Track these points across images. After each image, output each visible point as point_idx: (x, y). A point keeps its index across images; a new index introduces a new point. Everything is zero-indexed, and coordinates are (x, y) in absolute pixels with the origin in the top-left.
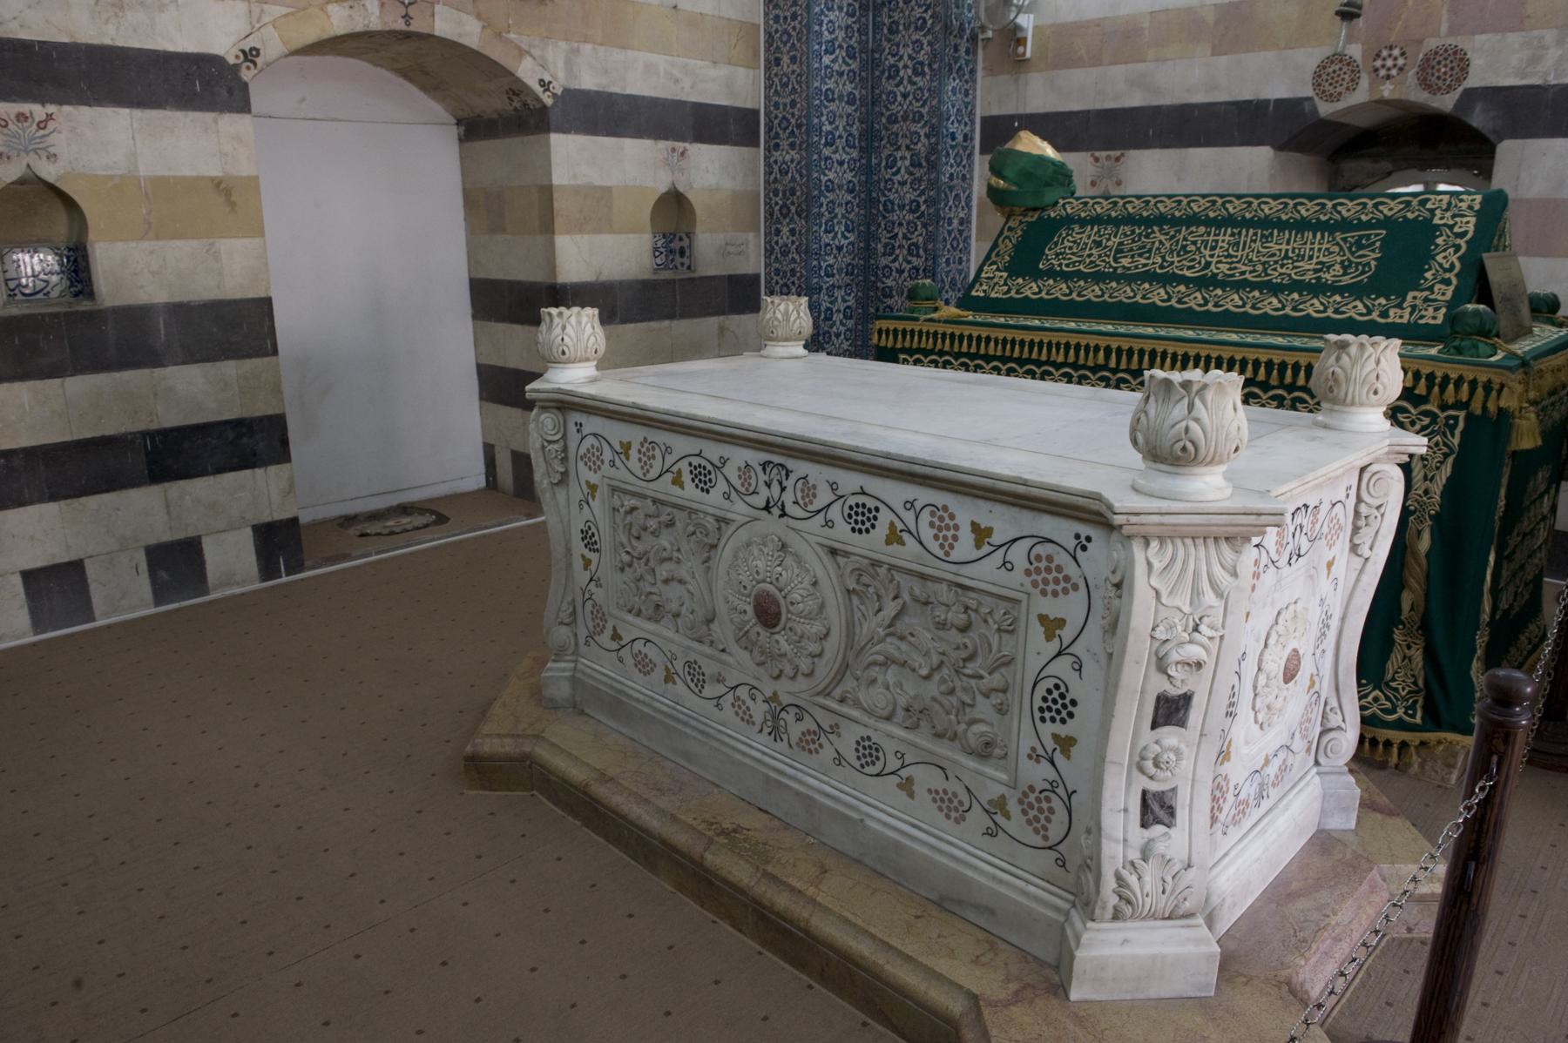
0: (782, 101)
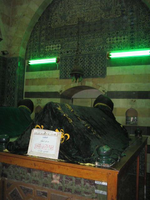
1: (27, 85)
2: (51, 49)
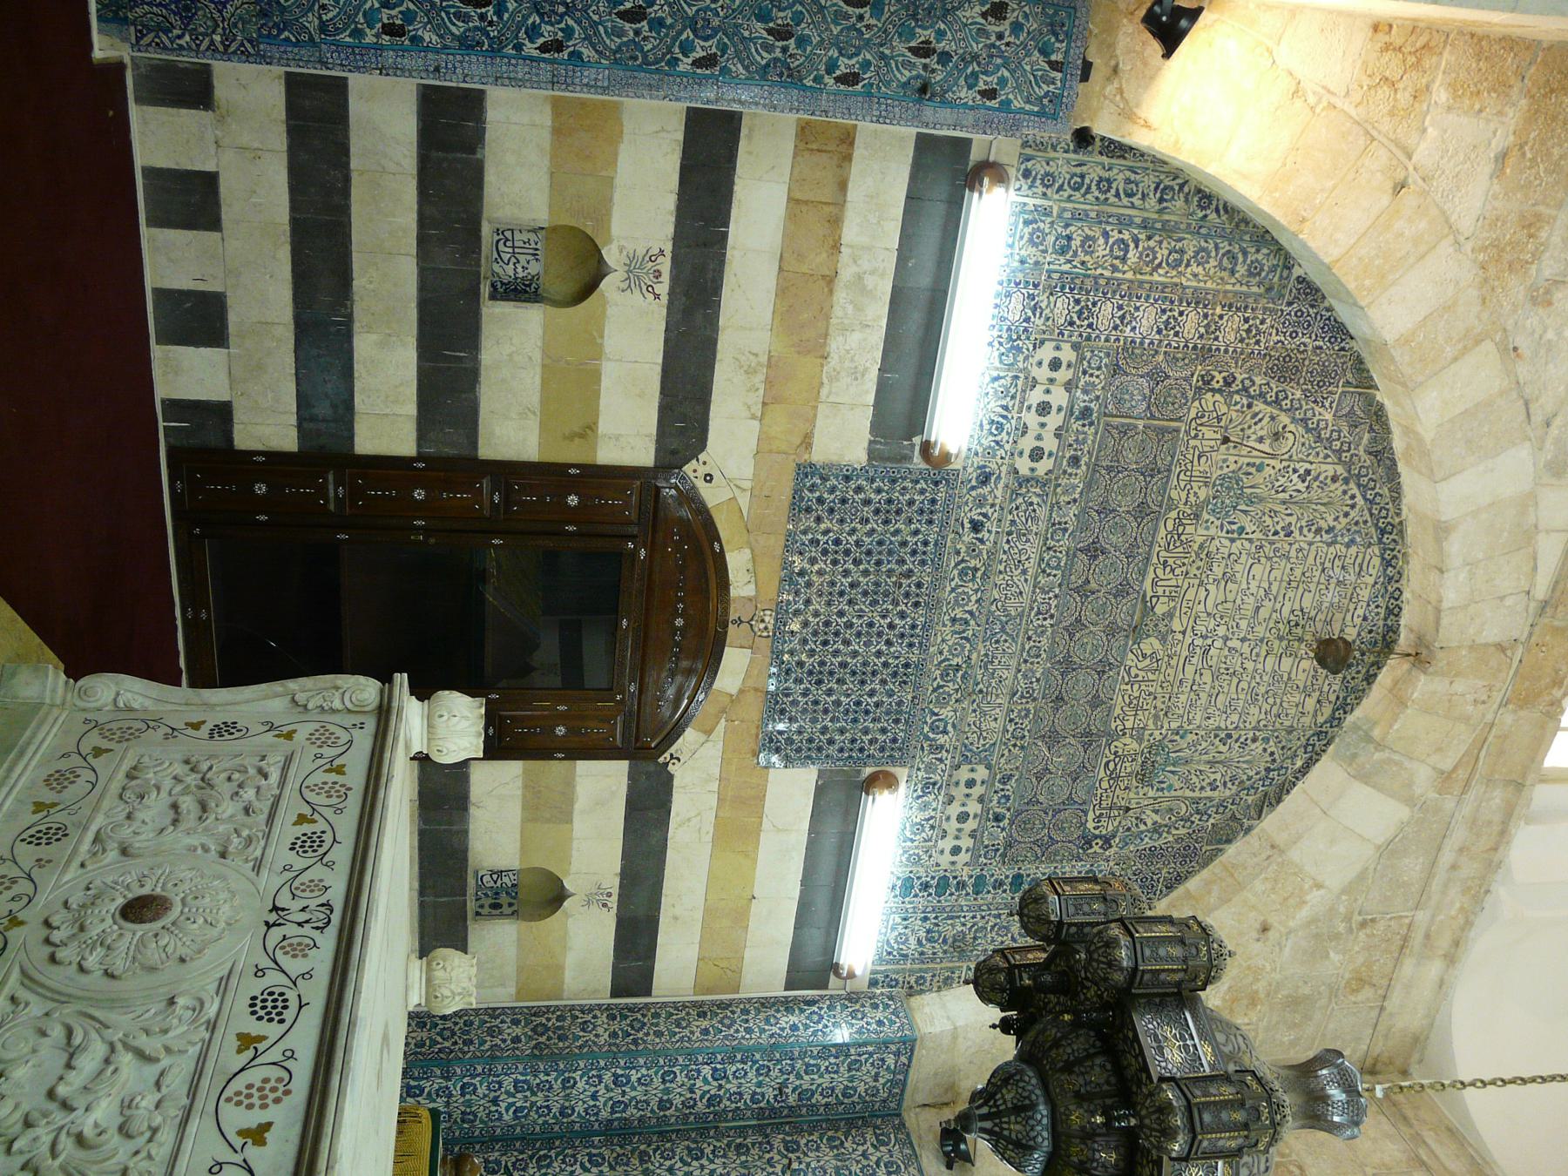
0: (662, 1020)
1: (804, 131)
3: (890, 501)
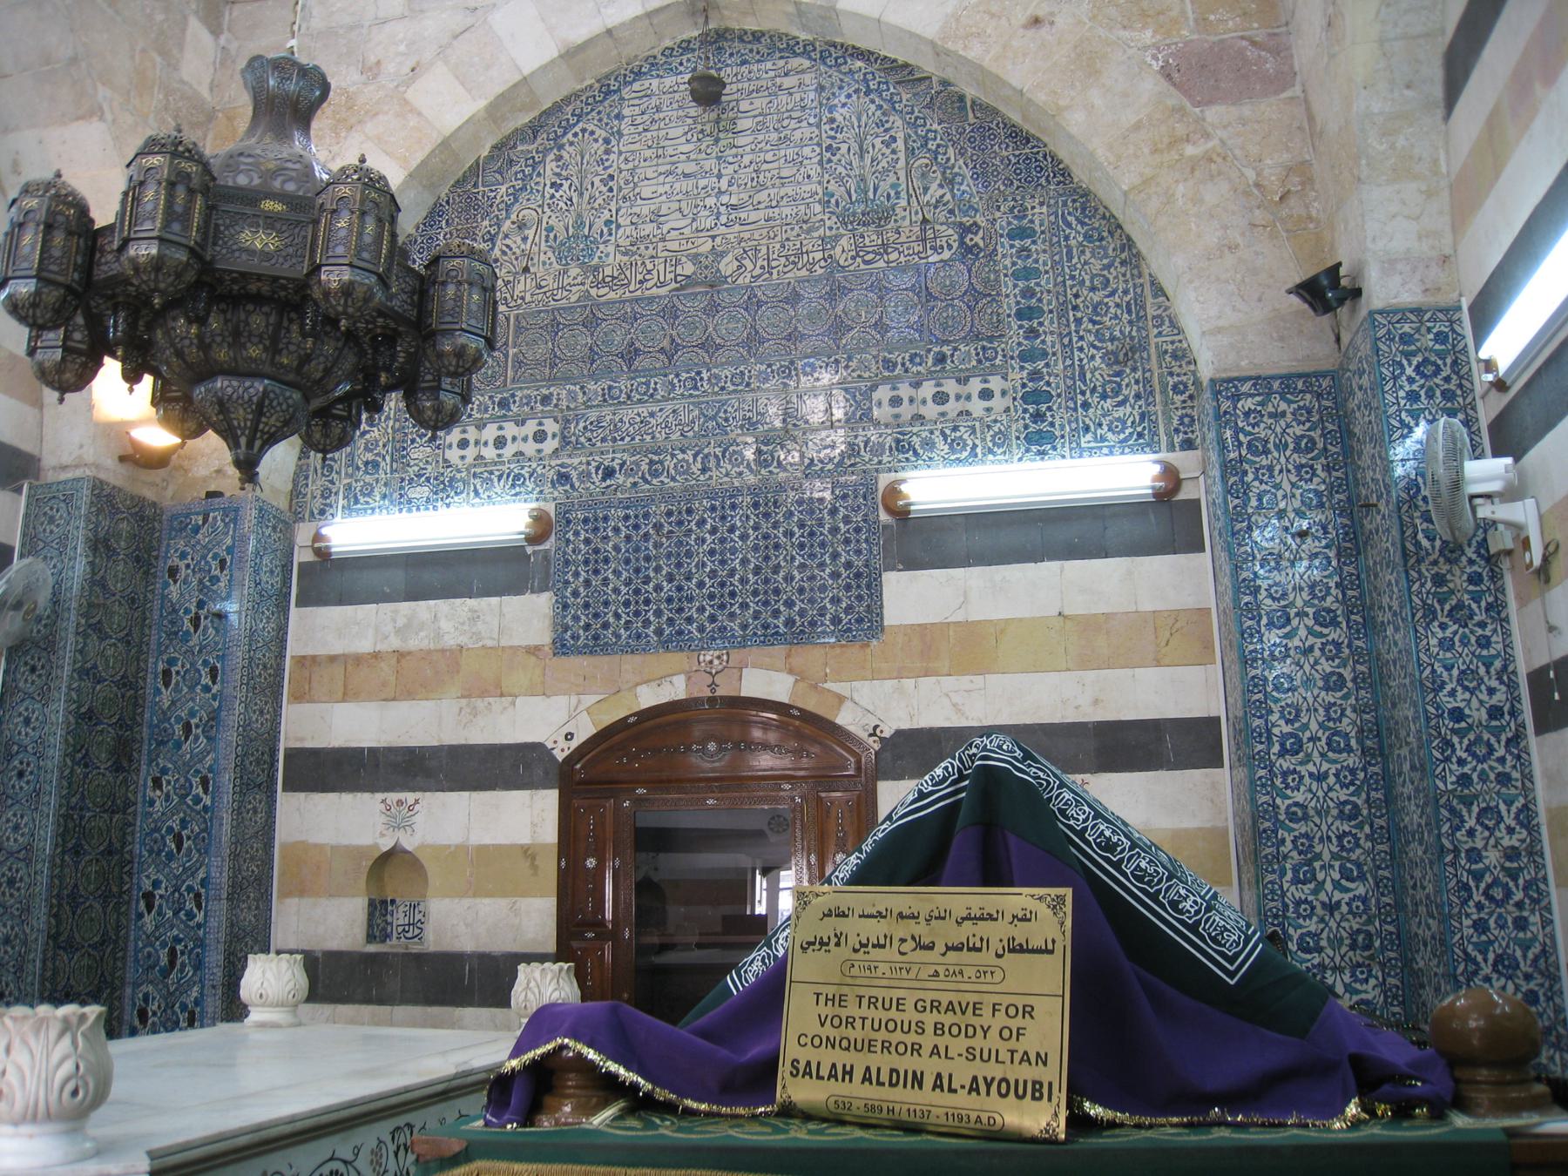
1: (298, 698)
2: (490, 453)
3: (586, 562)
